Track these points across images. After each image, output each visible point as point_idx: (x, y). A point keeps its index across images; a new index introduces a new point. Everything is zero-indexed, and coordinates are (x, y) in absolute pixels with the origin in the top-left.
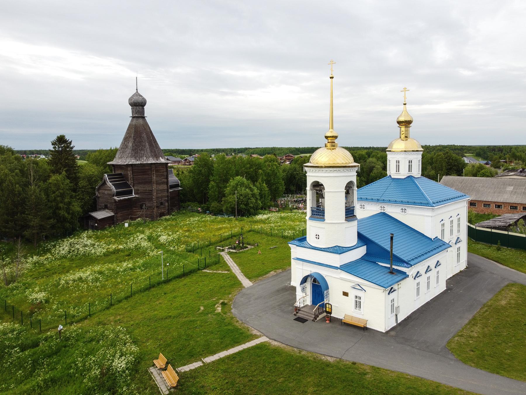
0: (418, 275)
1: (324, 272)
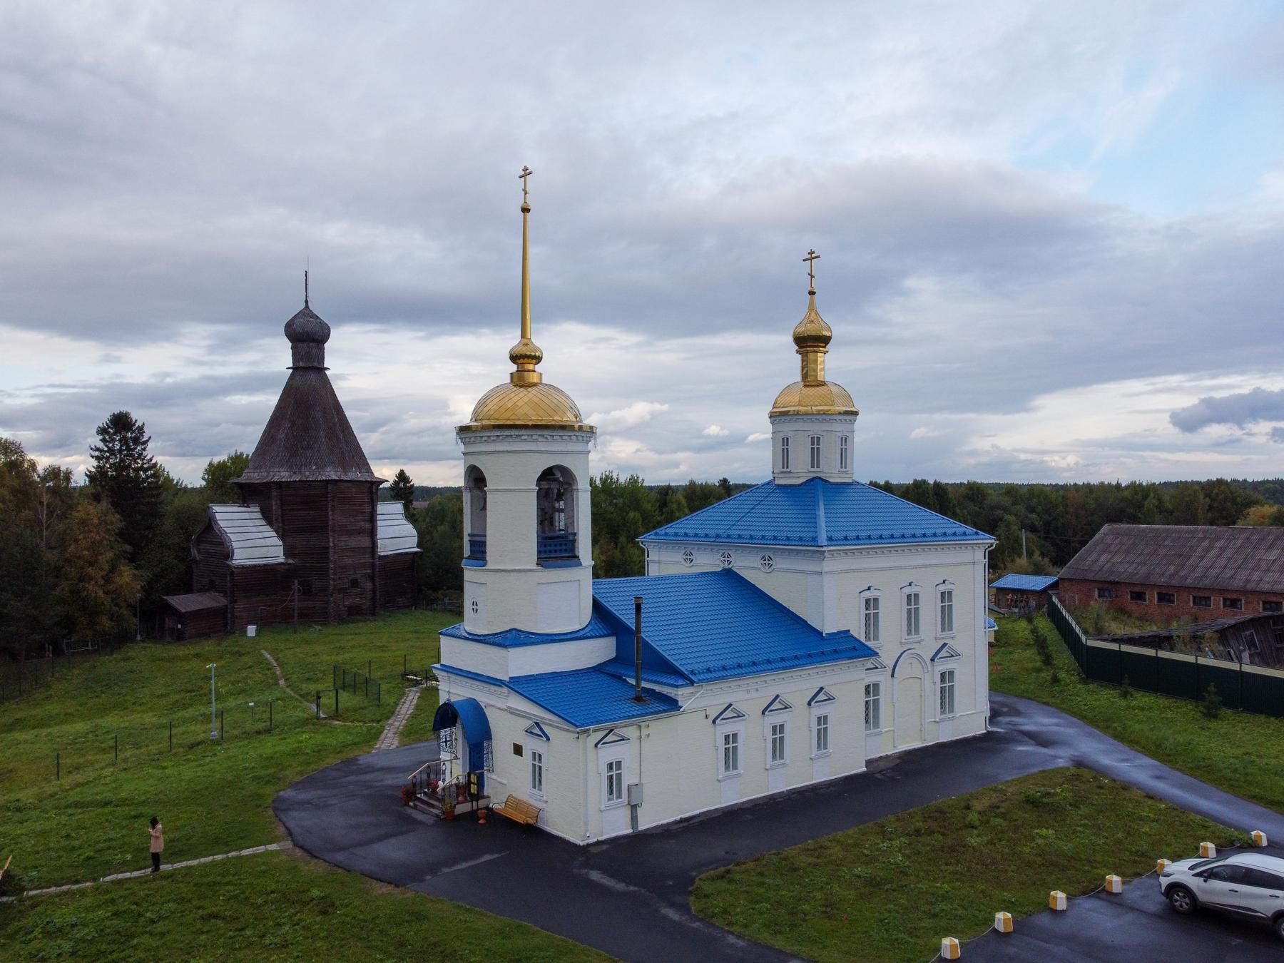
0: (729, 712)
1: (483, 696)
